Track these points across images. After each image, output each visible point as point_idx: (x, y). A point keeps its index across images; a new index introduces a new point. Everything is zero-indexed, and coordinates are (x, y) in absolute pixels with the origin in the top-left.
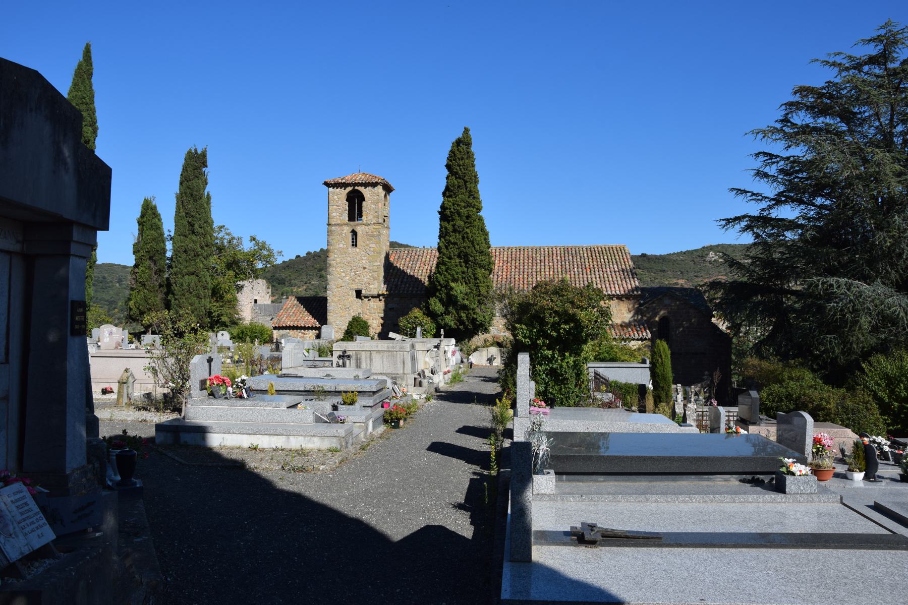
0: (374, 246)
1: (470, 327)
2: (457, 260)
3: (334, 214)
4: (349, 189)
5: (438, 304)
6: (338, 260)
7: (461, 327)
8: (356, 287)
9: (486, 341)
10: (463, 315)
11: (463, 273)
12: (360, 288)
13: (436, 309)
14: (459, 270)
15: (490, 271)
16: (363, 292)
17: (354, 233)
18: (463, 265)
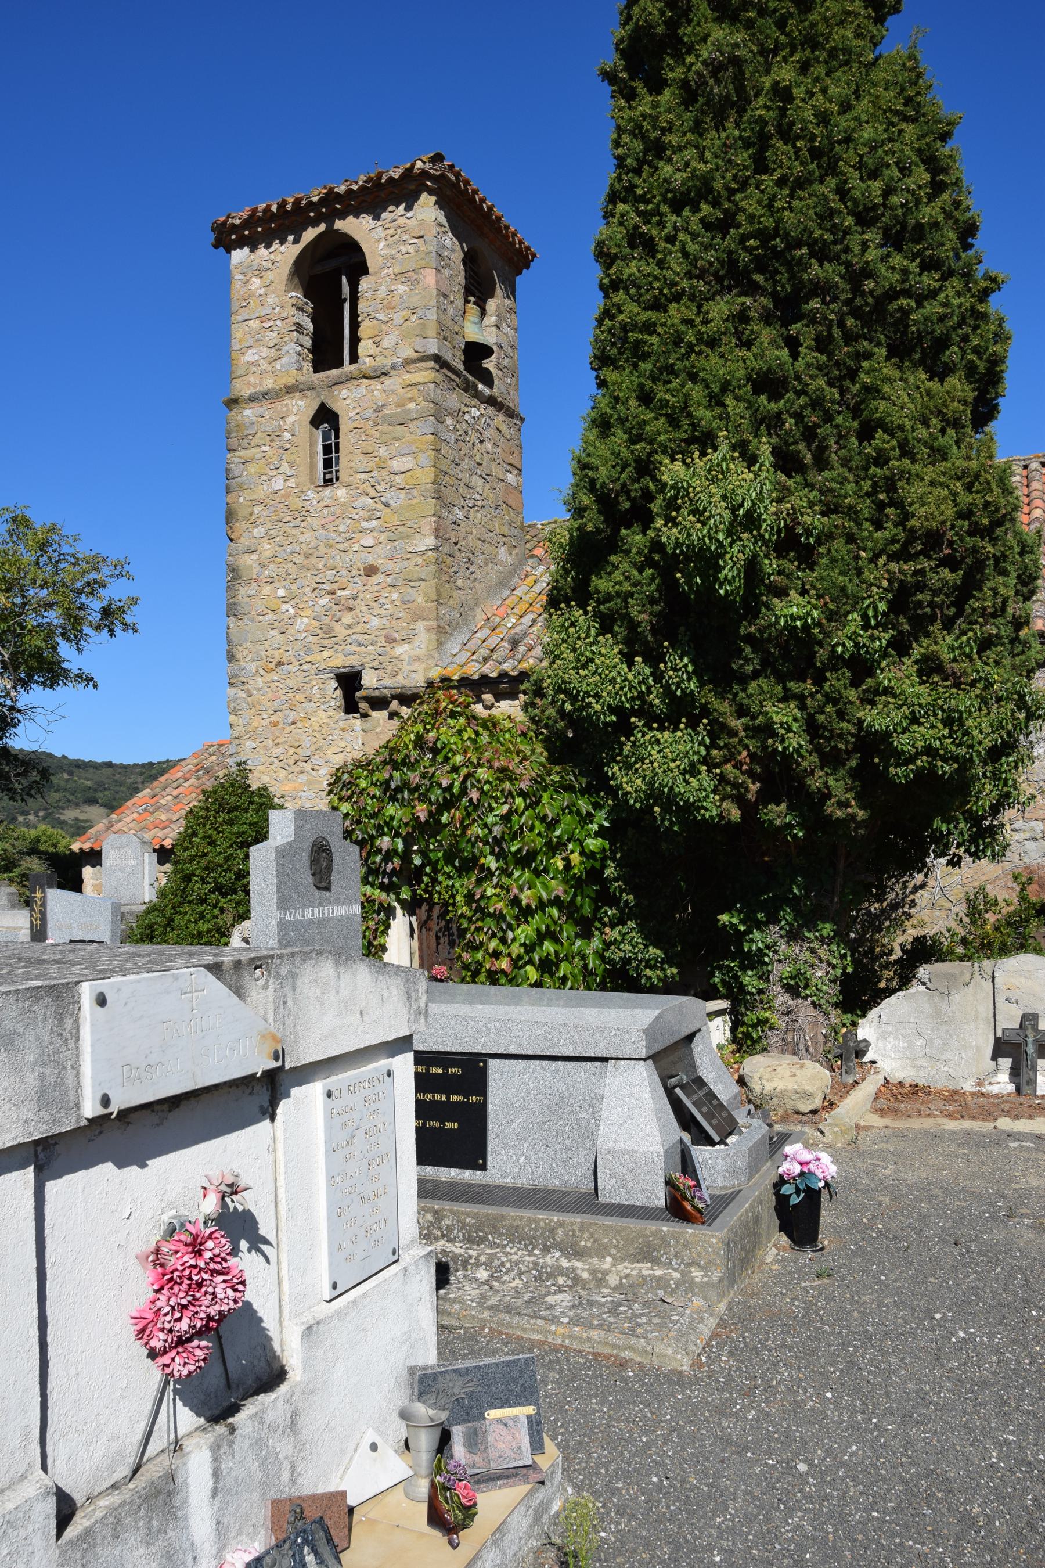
1: (840, 796)
3: (250, 356)
4: (310, 234)
5: (608, 651)
6: (267, 548)
7: (778, 813)
8: (339, 662)
9: (976, 906)
10: (782, 714)
11: (769, 383)
12: (354, 662)
14: (729, 364)
15: (987, 382)
16: (369, 680)
17: (325, 417)
18: (766, 335)
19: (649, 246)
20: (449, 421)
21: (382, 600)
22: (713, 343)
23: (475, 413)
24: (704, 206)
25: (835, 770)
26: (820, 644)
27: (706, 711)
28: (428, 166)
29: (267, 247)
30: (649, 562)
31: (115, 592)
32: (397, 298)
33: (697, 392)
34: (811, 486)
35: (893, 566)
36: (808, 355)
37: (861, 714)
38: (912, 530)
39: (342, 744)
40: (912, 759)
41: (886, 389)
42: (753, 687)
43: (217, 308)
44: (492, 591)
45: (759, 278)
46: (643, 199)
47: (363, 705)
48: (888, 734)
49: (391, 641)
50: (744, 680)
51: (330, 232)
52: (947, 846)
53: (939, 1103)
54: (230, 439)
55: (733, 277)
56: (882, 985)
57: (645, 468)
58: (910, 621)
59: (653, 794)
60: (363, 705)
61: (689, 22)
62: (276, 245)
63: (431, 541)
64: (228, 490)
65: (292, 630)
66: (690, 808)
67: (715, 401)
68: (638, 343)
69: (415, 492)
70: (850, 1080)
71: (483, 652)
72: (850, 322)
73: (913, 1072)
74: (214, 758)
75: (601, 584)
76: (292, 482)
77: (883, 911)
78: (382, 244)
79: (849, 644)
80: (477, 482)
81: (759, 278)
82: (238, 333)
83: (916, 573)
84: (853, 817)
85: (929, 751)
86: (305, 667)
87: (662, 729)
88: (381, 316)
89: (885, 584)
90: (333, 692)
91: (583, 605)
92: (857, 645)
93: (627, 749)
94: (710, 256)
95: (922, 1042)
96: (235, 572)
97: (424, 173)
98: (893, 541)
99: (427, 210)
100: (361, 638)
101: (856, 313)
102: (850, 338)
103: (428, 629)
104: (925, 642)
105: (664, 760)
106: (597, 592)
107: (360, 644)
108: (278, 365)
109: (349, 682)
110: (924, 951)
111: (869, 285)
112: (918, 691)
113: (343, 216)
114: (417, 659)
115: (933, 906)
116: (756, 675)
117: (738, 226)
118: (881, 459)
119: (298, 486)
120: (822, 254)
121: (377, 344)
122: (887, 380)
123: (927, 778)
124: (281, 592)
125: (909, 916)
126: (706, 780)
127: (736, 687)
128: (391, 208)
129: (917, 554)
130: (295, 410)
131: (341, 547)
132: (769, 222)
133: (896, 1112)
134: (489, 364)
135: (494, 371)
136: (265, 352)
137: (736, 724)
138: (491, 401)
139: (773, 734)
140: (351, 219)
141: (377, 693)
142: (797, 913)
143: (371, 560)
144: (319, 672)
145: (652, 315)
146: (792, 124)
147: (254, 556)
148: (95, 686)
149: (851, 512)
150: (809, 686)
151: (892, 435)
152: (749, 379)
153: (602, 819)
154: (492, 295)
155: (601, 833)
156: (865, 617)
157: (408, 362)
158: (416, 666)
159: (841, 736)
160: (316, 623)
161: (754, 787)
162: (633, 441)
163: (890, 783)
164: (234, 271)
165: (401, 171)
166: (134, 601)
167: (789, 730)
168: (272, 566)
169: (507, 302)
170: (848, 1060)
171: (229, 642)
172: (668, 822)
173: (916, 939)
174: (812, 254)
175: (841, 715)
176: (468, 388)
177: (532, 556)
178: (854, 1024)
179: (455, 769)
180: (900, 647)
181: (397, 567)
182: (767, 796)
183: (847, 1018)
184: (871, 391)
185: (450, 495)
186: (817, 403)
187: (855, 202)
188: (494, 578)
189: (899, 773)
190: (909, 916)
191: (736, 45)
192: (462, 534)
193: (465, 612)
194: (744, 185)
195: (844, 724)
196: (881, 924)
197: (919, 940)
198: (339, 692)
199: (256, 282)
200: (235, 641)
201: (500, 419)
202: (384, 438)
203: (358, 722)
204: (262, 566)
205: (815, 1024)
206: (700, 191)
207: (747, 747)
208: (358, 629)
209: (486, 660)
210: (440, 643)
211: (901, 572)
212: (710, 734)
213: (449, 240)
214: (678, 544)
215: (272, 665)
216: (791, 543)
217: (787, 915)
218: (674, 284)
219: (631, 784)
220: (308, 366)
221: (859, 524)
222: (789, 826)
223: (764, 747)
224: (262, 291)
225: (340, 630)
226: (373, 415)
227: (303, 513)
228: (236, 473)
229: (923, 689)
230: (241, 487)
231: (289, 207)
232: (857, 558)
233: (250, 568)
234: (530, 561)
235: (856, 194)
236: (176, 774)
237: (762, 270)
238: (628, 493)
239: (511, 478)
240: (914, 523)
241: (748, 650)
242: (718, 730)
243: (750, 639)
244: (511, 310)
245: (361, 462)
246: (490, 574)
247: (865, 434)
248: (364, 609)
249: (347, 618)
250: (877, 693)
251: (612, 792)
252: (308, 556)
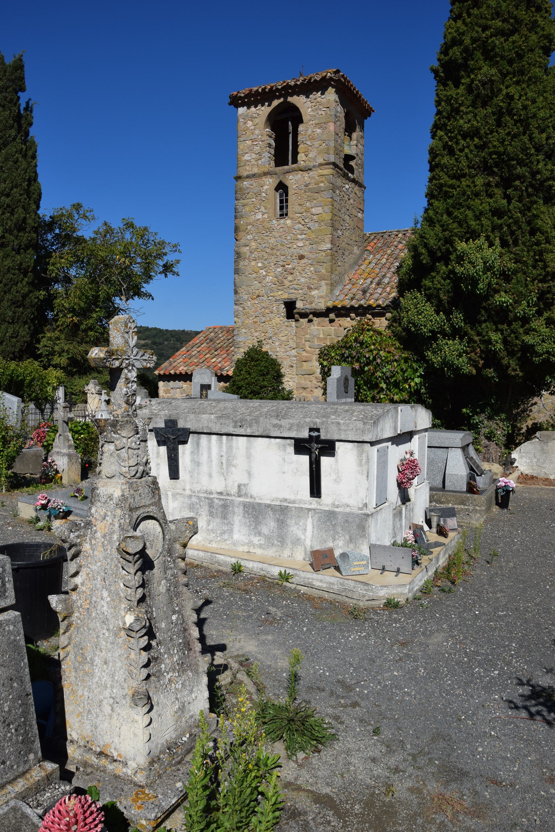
0: (319, 210)
2: (480, 181)
3: (247, 157)
4: (276, 103)
5: (429, 309)
6: (253, 244)
7: (490, 372)
8: (286, 296)
10: (495, 337)
11: (497, 213)
12: (293, 297)
13: (420, 320)
14: (483, 204)
17: (282, 188)
18: (498, 192)
19: (451, 152)
20: (338, 192)
21: (306, 270)
22: (477, 195)
23: (347, 186)
24: (476, 139)
25: (512, 357)
26: (511, 312)
27: (466, 334)
28: (333, 75)
29: (256, 107)
30: (448, 277)
31: (170, 258)
32: (316, 135)
33: (470, 213)
34: (511, 253)
35: (540, 285)
36: (515, 203)
37: (524, 338)
38: (548, 272)
39: (286, 332)
40: (541, 355)
41: (542, 216)
42: (484, 325)
43: (232, 135)
44: (351, 267)
45: (496, 170)
46: (450, 131)
47: (297, 316)
48: (534, 346)
49: (310, 288)
50: (480, 323)
51: (285, 101)
52: (550, 387)
53: (541, 481)
54: (238, 194)
55: (486, 168)
56: (517, 441)
57: (449, 241)
58: (544, 304)
59: (445, 363)
60: (297, 316)
61: (473, 59)
62: (259, 107)
63: (329, 246)
64: (236, 217)
65: (264, 282)
66: (458, 369)
67: (477, 218)
68: (446, 192)
69: (322, 224)
70: (508, 472)
71: (351, 295)
72: (530, 190)
73: (532, 471)
74: (212, 334)
75: (427, 283)
76: (266, 216)
77: (518, 413)
78: (310, 110)
79: (522, 312)
80: (347, 218)
81: (496, 170)
82: (241, 146)
83: (548, 287)
84: (518, 375)
85: (548, 352)
86: (270, 298)
87: (449, 339)
88: (309, 143)
89: (536, 291)
90: (282, 309)
91: (419, 291)
92: (524, 313)
93: (434, 346)
94: (477, 160)
95: (536, 460)
96: (238, 255)
97: (331, 78)
98: (540, 275)
99: (331, 95)
100: (296, 287)
101: (532, 185)
102: (529, 195)
103: (327, 284)
104: (549, 312)
105: (451, 350)
106: (425, 285)
107: (295, 289)
108: (260, 162)
109: (290, 306)
110: (536, 428)
111: (539, 176)
112: (544, 330)
113: (292, 96)
114: (322, 297)
115: (539, 412)
116: (485, 321)
117: (489, 148)
118: (538, 243)
119: (268, 217)
120: (521, 163)
121: (306, 156)
122: (543, 213)
123: (546, 362)
124: (260, 265)
125: (529, 416)
126: (464, 359)
127: (477, 325)
128: (314, 93)
129: (549, 280)
130: (268, 183)
131: (288, 246)
132: (501, 149)
133: (526, 483)
134: (352, 163)
135: (354, 166)
136: (254, 156)
137: (476, 338)
138: (354, 181)
139: (491, 343)
140: (295, 97)
141: (303, 311)
142: (492, 409)
143: (301, 252)
144: (276, 301)
145: (453, 182)
146: (513, 109)
147: (248, 248)
148: (153, 299)
149: (525, 263)
150: (505, 327)
151: (543, 234)
152: (490, 210)
153: (421, 371)
154: (354, 131)
155: (421, 376)
156: (528, 303)
157: (321, 165)
158: (321, 300)
159: (516, 345)
160: (275, 279)
161: (482, 362)
162: (444, 231)
163: (533, 363)
164: (240, 118)
165: (320, 77)
166: (178, 262)
167: (497, 342)
168: (256, 253)
169: (361, 133)
170: (508, 465)
171: (235, 285)
172: (449, 374)
173: (534, 424)
174: (518, 163)
175: (517, 338)
176: (345, 176)
177: (367, 250)
178: (510, 453)
179: (371, 351)
180: (539, 313)
181: (313, 256)
182: (485, 366)
183: (507, 451)
184: (536, 216)
185: (337, 225)
186: (516, 222)
187: (536, 143)
188: (352, 261)
189: (536, 359)
190: (529, 416)
191: (492, 75)
192: (341, 242)
193: (341, 276)
194: (492, 132)
195: (518, 341)
196: (517, 418)
197: (535, 424)
198: (285, 310)
199: (250, 123)
200: (238, 285)
201: (357, 188)
202: (309, 198)
203: (294, 323)
204: (251, 252)
205: (496, 451)
206: (474, 133)
207: (480, 348)
208: (295, 282)
209: (352, 299)
210: (332, 290)
211: (543, 287)
212: (468, 343)
213: (340, 108)
214: (462, 273)
215: (255, 297)
216: (506, 276)
217: (488, 410)
218: (462, 170)
219: (436, 360)
220: (273, 163)
221: (527, 267)
222: (493, 377)
223: (487, 348)
224: (253, 128)
225: (286, 283)
226: (304, 188)
227: (270, 230)
228: (240, 210)
229: (547, 330)
230: (242, 217)
231: (267, 90)
232: (526, 280)
233: (245, 253)
234: (366, 252)
235: (537, 140)
236: (196, 340)
237: (497, 166)
238: (441, 250)
239: (360, 215)
240: (549, 269)
241: (483, 312)
242: (470, 341)
243: (484, 308)
244: (362, 137)
245: (297, 208)
246: (349, 259)
247: (532, 233)
248: (298, 274)
249: (290, 278)
250: (530, 330)
251: (427, 362)
252: (272, 249)
